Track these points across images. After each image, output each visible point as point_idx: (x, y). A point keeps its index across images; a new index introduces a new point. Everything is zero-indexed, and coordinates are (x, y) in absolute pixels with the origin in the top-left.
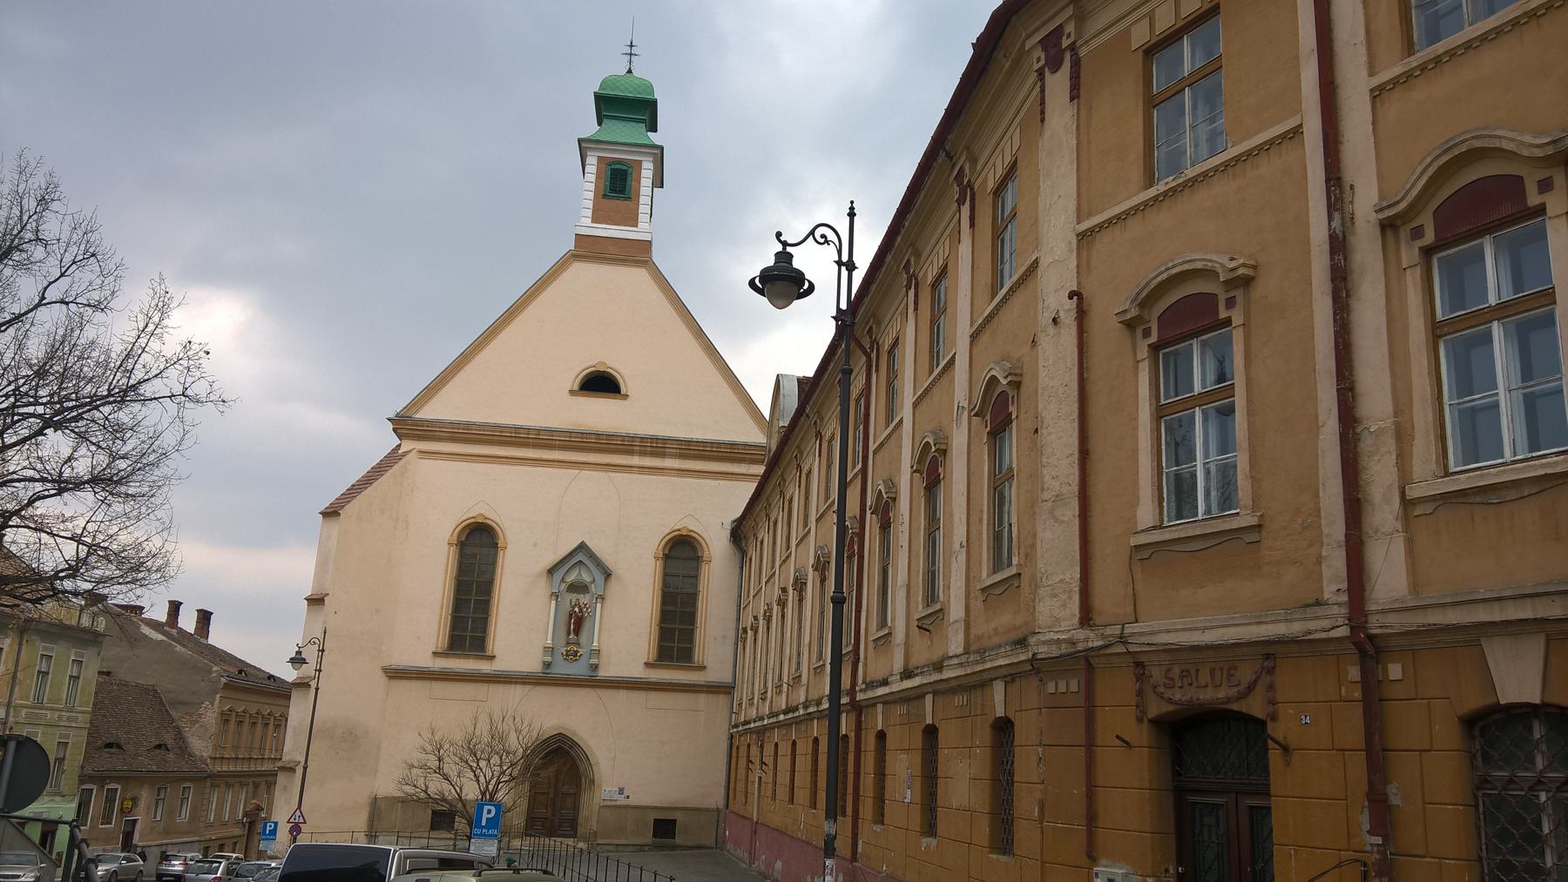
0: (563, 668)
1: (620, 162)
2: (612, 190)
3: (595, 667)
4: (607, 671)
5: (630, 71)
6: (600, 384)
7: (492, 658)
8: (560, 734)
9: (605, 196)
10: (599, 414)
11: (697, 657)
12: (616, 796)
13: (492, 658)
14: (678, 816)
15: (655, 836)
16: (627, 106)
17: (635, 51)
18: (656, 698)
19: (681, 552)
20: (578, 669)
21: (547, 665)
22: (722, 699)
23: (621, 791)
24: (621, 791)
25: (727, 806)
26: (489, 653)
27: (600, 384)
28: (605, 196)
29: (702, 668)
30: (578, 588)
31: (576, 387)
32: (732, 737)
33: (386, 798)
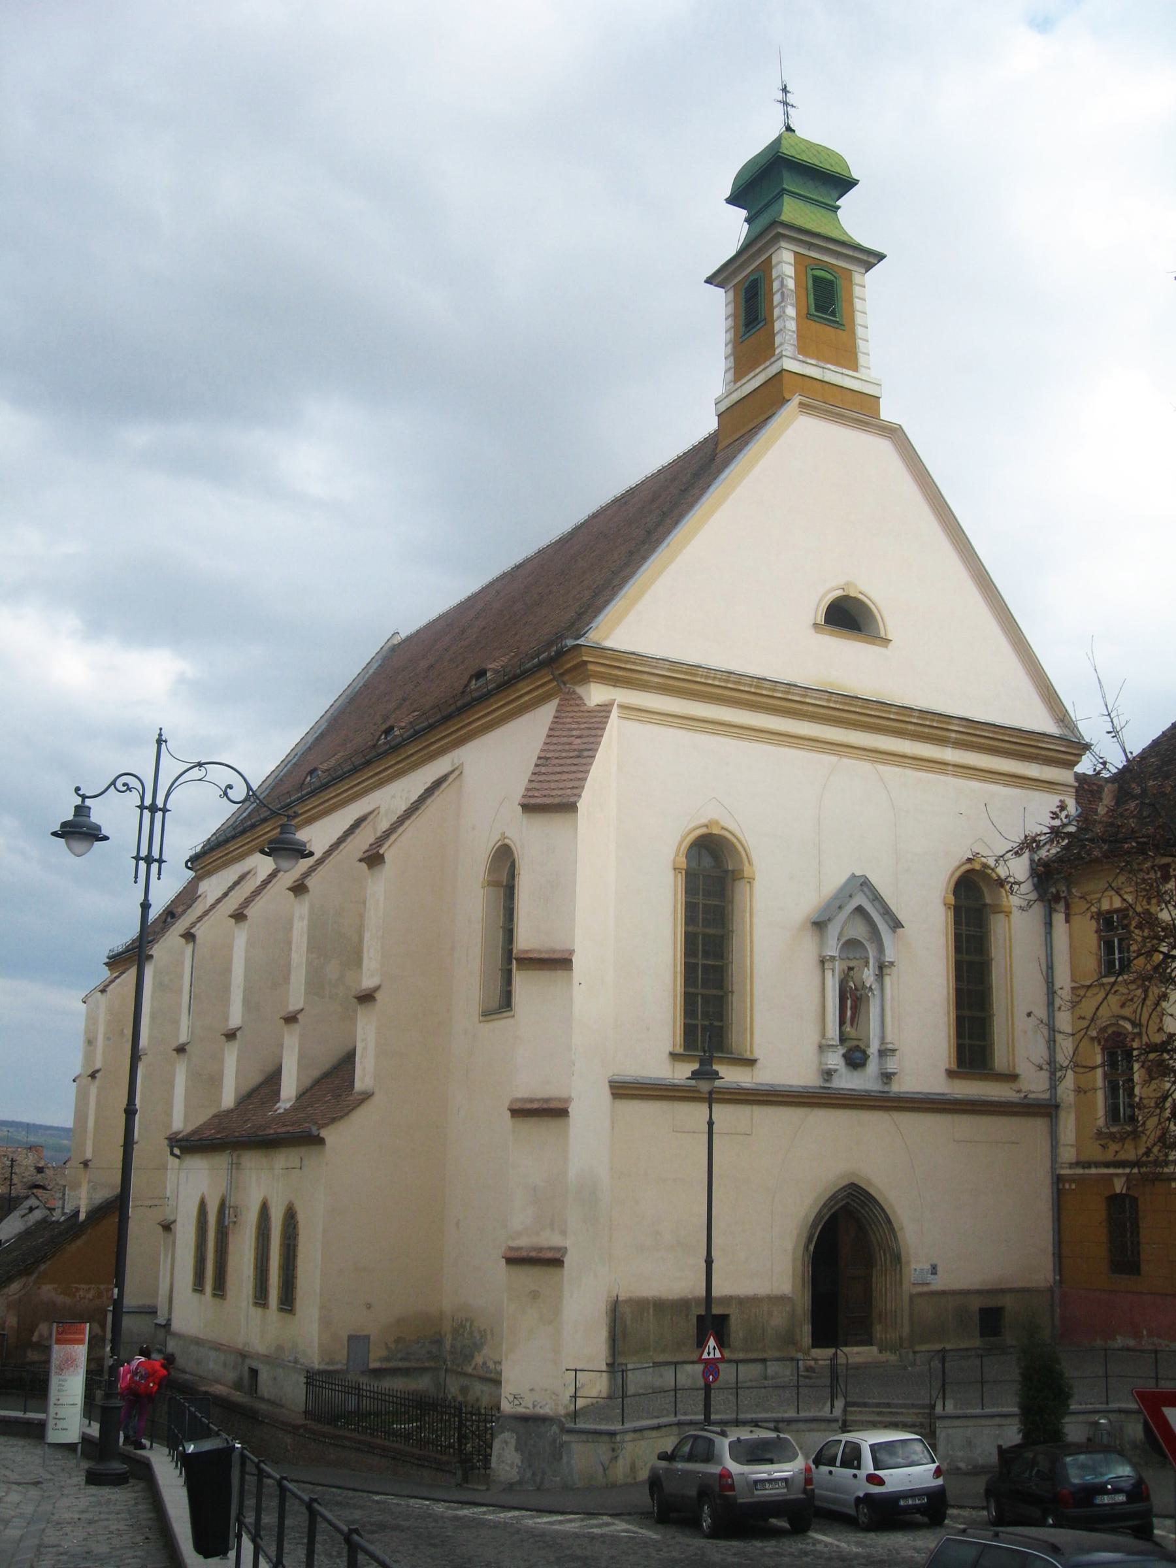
0: (848, 1081)
1: (824, 266)
2: (819, 308)
3: (887, 1077)
4: (906, 1084)
5: (789, 129)
6: (847, 616)
7: (751, 1062)
8: (853, 1184)
9: (809, 316)
10: (845, 665)
11: (1000, 1061)
12: (930, 1278)
13: (751, 1062)
14: (1008, 1302)
15: (982, 1335)
16: (785, 184)
17: (791, 99)
18: (964, 1124)
19: (972, 897)
20: (864, 1081)
21: (828, 1074)
22: (1038, 1126)
23: (934, 1270)
24: (934, 1270)
25: (1061, 1282)
26: (748, 1055)
27: (847, 616)
28: (809, 316)
29: (1013, 1077)
30: (851, 944)
31: (821, 619)
32: (1058, 1180)
33: (631, 1302)
